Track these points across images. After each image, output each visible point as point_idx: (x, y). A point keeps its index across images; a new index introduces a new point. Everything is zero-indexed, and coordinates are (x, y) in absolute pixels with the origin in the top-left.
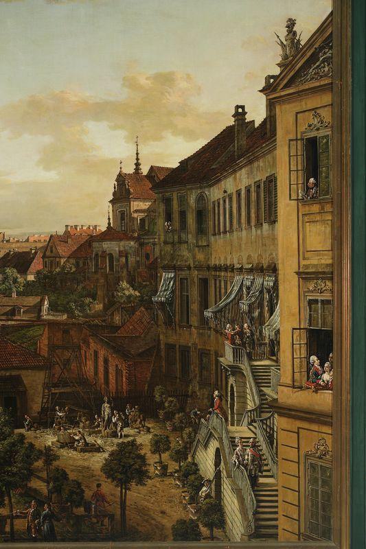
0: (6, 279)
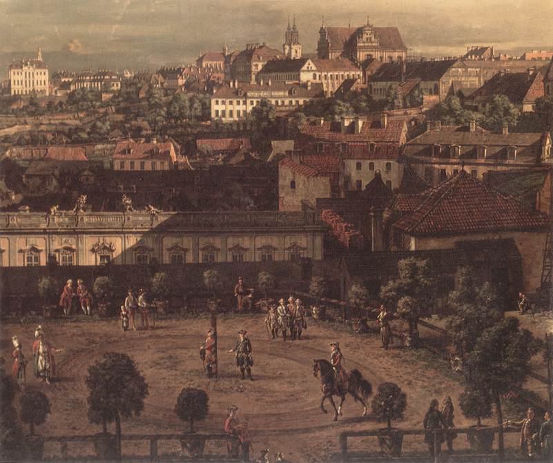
0: (495, 108)
